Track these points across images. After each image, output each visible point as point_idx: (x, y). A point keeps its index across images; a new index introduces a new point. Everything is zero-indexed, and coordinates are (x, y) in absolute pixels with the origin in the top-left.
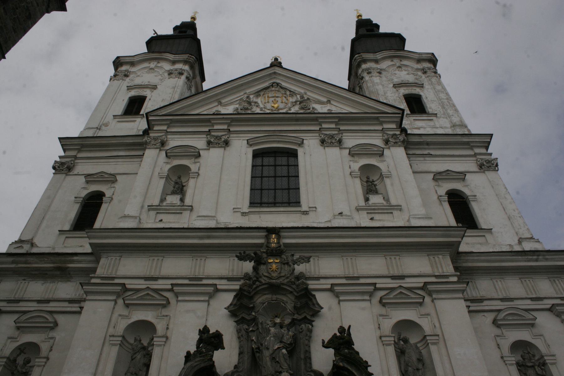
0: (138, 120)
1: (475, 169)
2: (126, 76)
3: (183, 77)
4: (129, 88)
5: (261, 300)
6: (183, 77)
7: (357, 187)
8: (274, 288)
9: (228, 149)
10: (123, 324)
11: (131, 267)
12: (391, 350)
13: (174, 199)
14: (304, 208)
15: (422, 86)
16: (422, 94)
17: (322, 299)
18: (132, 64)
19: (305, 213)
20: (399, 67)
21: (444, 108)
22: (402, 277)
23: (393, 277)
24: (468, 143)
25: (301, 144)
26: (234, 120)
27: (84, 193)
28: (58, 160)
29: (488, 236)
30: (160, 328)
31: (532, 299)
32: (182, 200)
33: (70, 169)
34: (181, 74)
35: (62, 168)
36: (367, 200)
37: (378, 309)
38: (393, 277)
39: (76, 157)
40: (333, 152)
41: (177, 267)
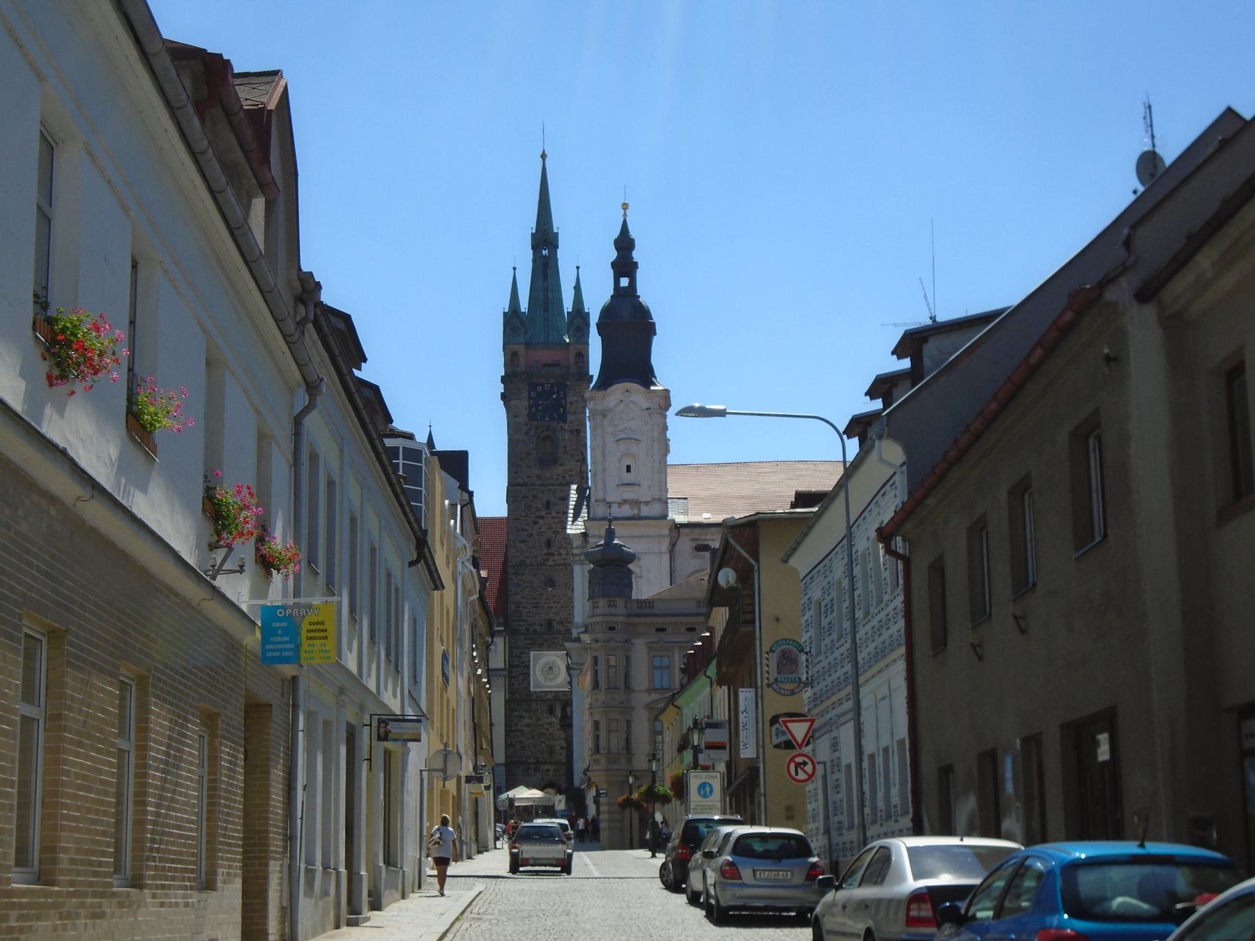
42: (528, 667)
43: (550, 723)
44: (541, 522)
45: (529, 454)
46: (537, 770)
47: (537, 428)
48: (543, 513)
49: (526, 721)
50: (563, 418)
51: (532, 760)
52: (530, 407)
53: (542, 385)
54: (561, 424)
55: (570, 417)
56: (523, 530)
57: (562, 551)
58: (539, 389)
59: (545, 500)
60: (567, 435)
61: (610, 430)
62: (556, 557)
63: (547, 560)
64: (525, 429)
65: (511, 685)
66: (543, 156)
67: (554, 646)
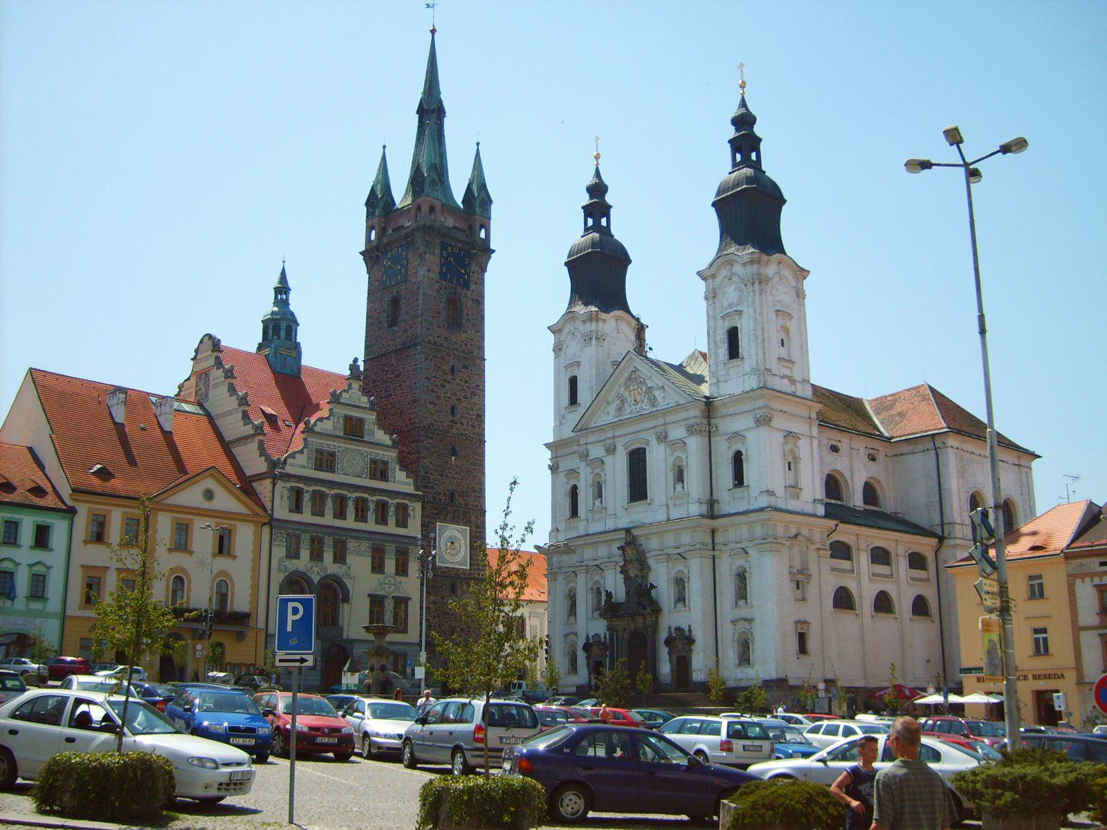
0: (578, 409)
1: (754, 425)
2: (560, 349)
5: (629, 566)
7: (671, 477)
8: (631, 561)
10: (591, 583)
11: (588, 554)
13: (598, 502)
14: (649, 501)
15: (740, 313)
16: (739, 326)
19: (650, 504)
21: (749, 344)
25: (647, 442)
26: (613, 426)
27: (568, 488)
30: (602, 583)
32: (602, 503)
33: (557, 469)
34: (591, 338)
35: (554, 469)
36: (675, 489)
37: (670, 566)
39: (556, 457)
40: (662, 446)
41: (603, 551)
44: (447, 386)
45: (439, 313)
50: (466, 285)
52: (442, 265)
53: (453, 247)
54: (465, 291)
55: (473, 287)
56: (433, 391)
58: (449, 249)
59: (451, 364)
60: (470, 302)
61: (770, 298)
62: (459, 426)
64: (437, 286)
66: (433, 32)
67: (455, 520)
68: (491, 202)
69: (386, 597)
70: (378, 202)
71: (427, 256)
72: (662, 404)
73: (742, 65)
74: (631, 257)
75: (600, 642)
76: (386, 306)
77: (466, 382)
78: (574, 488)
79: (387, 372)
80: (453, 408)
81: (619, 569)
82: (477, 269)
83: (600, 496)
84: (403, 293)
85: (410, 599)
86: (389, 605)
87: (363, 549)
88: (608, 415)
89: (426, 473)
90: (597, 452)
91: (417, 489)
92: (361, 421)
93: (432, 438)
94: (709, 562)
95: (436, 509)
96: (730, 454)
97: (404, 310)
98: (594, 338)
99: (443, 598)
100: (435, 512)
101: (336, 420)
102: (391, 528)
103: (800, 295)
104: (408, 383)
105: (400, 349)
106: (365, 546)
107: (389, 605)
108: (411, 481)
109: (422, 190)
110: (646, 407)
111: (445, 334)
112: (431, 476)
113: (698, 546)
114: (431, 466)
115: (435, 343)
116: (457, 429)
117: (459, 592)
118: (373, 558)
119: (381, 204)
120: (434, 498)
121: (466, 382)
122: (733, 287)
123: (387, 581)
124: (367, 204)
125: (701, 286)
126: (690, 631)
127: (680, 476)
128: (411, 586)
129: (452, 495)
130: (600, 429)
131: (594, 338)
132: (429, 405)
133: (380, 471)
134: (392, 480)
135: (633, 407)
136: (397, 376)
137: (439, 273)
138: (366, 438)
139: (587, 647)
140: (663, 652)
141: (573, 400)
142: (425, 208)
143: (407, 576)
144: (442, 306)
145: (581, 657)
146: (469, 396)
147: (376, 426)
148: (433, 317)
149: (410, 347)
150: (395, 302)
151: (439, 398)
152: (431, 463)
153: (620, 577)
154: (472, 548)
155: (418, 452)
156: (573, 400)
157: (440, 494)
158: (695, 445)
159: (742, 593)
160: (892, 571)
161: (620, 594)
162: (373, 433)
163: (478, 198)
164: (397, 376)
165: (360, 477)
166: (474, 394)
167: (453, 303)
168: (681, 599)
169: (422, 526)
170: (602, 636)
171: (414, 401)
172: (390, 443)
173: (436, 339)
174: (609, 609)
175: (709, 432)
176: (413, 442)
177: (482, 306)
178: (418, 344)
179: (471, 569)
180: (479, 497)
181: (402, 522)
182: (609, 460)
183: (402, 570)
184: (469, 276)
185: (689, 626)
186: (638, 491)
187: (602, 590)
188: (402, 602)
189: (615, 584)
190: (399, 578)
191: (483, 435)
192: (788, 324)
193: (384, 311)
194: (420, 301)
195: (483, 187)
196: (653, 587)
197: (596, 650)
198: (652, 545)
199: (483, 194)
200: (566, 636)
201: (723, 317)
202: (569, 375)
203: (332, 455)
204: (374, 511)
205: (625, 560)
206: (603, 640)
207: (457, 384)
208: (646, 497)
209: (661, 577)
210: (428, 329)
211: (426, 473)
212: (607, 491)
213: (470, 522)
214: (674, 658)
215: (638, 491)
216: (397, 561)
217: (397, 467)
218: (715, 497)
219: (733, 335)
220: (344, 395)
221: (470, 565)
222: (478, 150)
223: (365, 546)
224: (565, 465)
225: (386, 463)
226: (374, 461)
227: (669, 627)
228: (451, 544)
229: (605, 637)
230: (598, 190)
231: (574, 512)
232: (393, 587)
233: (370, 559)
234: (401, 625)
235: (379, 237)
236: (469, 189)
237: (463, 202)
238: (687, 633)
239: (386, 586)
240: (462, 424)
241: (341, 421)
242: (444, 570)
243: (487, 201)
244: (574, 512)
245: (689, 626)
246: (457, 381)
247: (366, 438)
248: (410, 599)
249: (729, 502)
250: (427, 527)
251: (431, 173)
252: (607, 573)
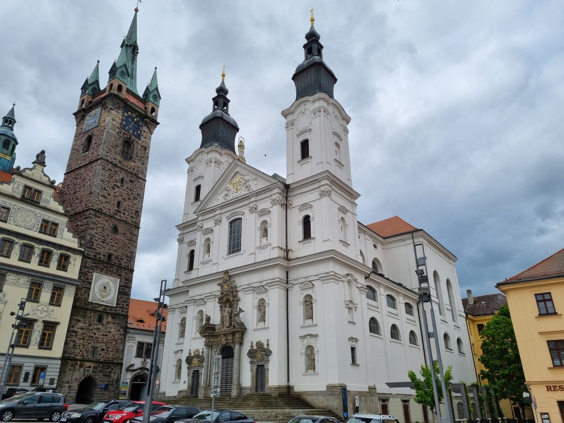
2: (192, 171)
3: (213, 164)
4: (195, 180)
6: (213, 164)
9: (222, 224)
12: (256, 311)
13: (206, 257)
17: (240, 295)
18: (193, 160)
20: (303, 113)
22: (262, 282)
23: (260, 282)
24: (317, 179)
27: (188, 252)
28: (178, 237)
29: (312, 241)
31: (315, 276)
35: (180, 241)
38: (260, 282)
39: (183, 234)
42: (90, 283)
43: (98, 329)
44: (117, 189)
45: (117, 146)
46: (81, 366)
47: (124, 134)
48: (119, 185)
49: (81, 324)
50: (138, 137)
51: (79, 357)
53: (132, 113)
54: (137, 139)
55: (142, 139)
56: (105, 189)
57: (125, 212)
59: (121, 177)
60: (140, 147)
63: (116, 214)
65: (76, 294)
67: (108, 272)
68: (160, 98)
69: (36, 320)
70: (90, 87)
71: (113, 112)
72: (255, 189)
73: (312, 11)
74: (239, 127)
75: (199, 355)
76: (83, 142)
77: (131, 190)
78: (193, 252)
79: (77, 179)
80: (119, 203)
81: (217, 300)
82: (147, 130)
83: (209, 251)
84: (94, 134)
85: (59, 323)
86: (38, 328)
87: (21, 282)
88: (220, 200)
89: (91, 238)
90: (209, 224)
91: (81, 245)
92: (40, 192)
93: (100, 217)
94: (284, 293)
95: (95, 263)
96: (301, 218)
97: (94, 141)
98: (213, 163)
99: (91, 325)
100: (94, 265)
101: (16, 186)
102: (52, 269)
103: (346, 131)
104: (89, 183)
105: (87, 164)
106: (24, 281)
107: (38, 328)
108: (76, 240)
109: (115, 75)
110: (243, 192)
111: (119, 158)
112: (95, 242)
113: (277, 280)
114: (96, 235)
115: (111, 163)
116: (120, 216)
117: (105, 321)
118: (31, 290)
119: (91, 88)
120: (95, 256)
121: (131, 190)
122: (306, 116)
123: (40, 308)
124: (82, 89)
125: (284, 121)
126: (268, 345)
127: (265, 233)
128: (62, 314)
129: (110, 256)
130: (213, 210)
131: (213, 163)
132: (100, 197)
133: (49, 227)
134: (60, 236)
135: (235, 194)
136: (83, 180)
137: (120, 124)
138: (42, 204)
139: (189, 360)
140: (246, 362)
141: (197, 198)
142: (115, 85)
143: (60, 306)
144: (119, 142)
145: (184, 366)
146: (131, 198)
147: (52, 199)
148: (112, 147)
149: (93, 162)
150: (90, 139)
151: (110, 195)
152: (97, 233)
153: (218, 306)
154: (119, 293)
155: (88, 224)
156: (197, 198)
157: (100, 254)
158: (277, 212)
159: (309, 316)
160: (397, 312)
161: (216, 320)
162: (48, 202)
163: (152, 94)
164: (83, 180)
165: (30, 229)
166: (135, 198)
167: (128, 143)
168: (262, 318)
169: (80, 273)
170: (201, 351)
171: (90, 193)
172: (63, 212)
173: (113, 160)
174: (208, 330)
175: (286, 205)
176: (85, 218)
177: (147, 151)
178: (98, 160)
179: (116, 307)
180: (130, 261)
181: (62, 266)
182: (216, 229)
183: (56, 301)
184: (141, 131)
185: (268, 341)
186: (235, 246)
187: (204, 317)
188: (50, 326)
189: (214, 312)
190: (51, 307)
191: (139, 224)
192: (339, 143)
193: (82, 145)
194: (104, 136)
195: (157, 89)
196: (241, 311)
197: (195, 361)
198: (241, 282)
199: (155, 93)
200: (176, 352)
201: (298, 136)
202: (196, 184)
203: (8, 209)
204: (38, 255)
205: (222, 293)
206: (201, 354)
207: (124, 190)
208: (239, 250)
209: (247, 304)
210: (107, 152)
211: (91, 238)
212: (213, 248)
213: (121, 276)
214: (255, 367)
215: (235, 246)
216: (53, 294)
217: (66, 229)
218: (289, 248)
219: (305, 145)
220: (27, 171)
221: (117, 304)
222: (155, 73)
223: (24, 281)
224: (188, 238)
225: (56, 225)
226: (45, 221)
227: (252, 343)
228: (104, 289)
229: (203, 352)
230: (222, 92)
231: (191, 267)
232: (45, 313)
233: (27, 290)
234: (46, 342)
235: (86, 106)
236: (147, 92)
237: (143, 96)
238: (265, 347)
239: (38, 312)
240: (124, 214)
241: (21, 188)
242: (94, 305)
243: (157, 97)
244: (191, 267)
245: (268, 341)
246: (125, 188)
247: (42, 204)
248: (59, 323)
249: (301, 250)
250: (85, 274)
251: (123, 71)
252: (208, 303)
